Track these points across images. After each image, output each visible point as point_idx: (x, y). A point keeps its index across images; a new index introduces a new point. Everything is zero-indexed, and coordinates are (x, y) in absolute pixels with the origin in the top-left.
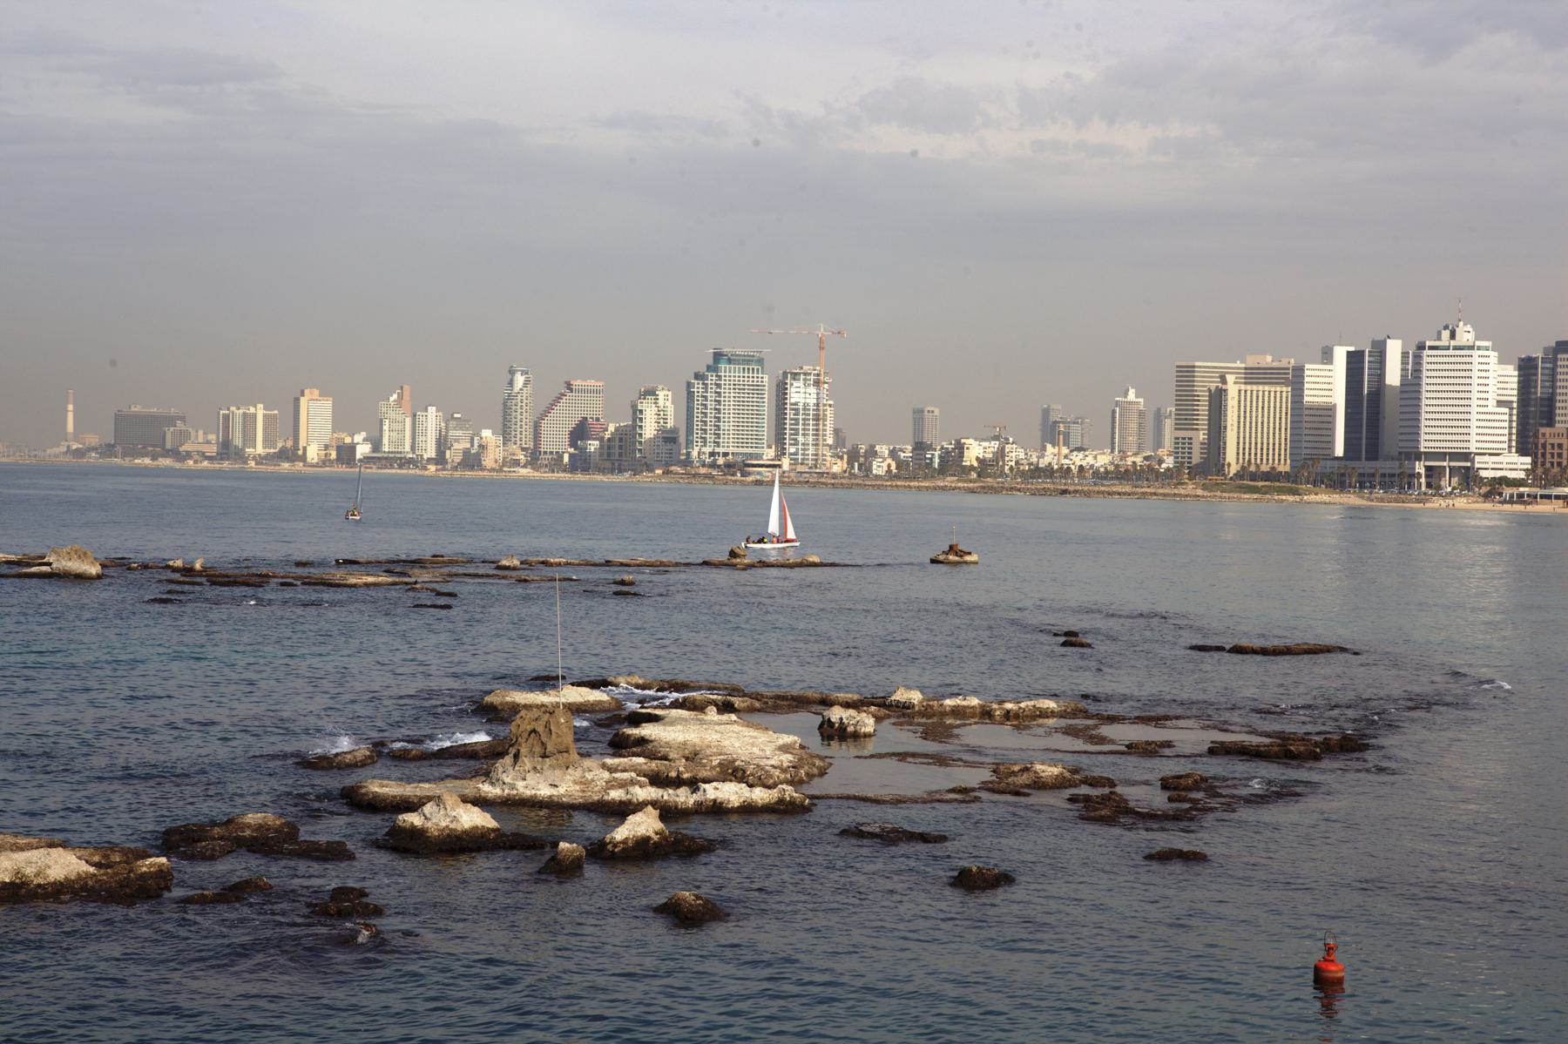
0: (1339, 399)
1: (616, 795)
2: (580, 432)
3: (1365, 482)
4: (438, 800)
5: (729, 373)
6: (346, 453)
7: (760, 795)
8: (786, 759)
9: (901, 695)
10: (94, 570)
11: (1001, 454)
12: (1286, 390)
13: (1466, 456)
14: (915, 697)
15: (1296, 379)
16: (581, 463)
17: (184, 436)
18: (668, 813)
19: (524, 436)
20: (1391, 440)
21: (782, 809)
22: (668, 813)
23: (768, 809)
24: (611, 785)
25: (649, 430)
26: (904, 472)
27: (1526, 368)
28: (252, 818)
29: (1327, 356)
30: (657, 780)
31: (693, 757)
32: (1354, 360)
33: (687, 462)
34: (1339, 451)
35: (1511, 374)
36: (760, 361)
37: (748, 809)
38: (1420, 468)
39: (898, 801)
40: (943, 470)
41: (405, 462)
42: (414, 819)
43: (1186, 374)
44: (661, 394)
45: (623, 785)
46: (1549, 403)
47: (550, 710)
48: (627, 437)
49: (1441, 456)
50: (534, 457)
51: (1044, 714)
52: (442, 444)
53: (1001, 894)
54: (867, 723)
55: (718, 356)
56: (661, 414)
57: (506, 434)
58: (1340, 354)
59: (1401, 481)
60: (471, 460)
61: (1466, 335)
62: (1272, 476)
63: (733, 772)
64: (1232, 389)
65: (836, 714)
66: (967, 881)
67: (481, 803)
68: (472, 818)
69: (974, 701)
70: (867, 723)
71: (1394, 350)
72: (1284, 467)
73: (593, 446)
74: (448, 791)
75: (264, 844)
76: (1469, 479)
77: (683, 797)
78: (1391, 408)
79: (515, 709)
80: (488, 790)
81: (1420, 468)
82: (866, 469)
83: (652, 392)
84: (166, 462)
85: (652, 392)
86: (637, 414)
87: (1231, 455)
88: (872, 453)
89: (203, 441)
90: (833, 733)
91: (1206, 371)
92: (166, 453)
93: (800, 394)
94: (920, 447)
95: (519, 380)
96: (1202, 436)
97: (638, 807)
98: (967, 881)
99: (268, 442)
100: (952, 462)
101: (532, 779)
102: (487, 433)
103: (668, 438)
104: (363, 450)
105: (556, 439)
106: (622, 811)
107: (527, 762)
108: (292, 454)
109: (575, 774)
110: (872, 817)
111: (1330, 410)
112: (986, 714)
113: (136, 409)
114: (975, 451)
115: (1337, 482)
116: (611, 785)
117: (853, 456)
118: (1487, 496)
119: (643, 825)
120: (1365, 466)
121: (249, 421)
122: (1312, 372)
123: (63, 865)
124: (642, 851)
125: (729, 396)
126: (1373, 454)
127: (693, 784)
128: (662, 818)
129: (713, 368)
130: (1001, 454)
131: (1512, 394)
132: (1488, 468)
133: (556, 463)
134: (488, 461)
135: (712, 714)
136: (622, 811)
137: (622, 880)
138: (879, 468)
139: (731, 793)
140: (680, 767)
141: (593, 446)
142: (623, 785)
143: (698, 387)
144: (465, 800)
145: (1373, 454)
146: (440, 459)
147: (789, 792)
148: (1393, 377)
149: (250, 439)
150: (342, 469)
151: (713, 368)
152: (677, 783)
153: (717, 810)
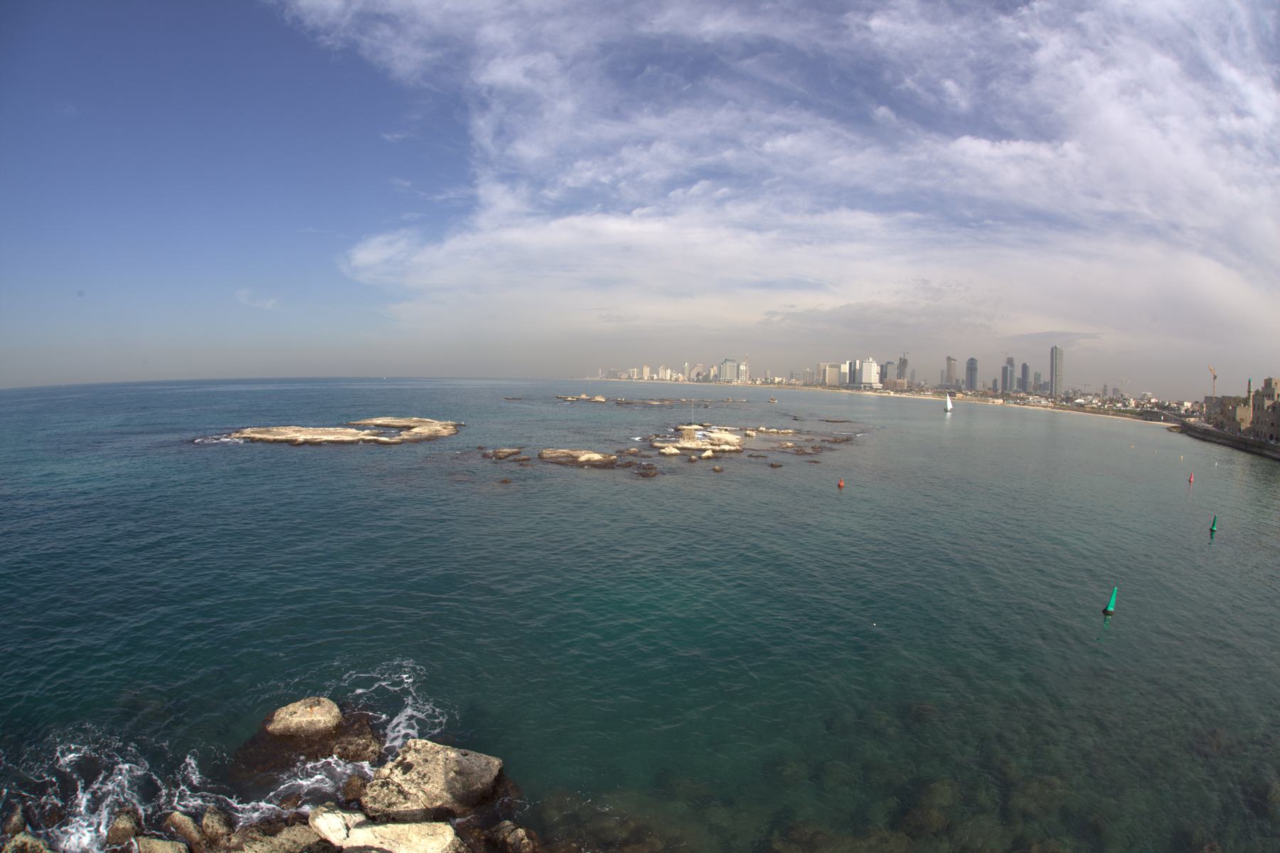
0: (848, 371)
1: (704, 447)
2: (698, 375)
3: (852, 388)
4: (668, 447)
5: (728, 363)
6: (652, 378)
7: (732, 448)
8: (738, 441)
9: (761, 429)
10: (604, 400)
11: (782, 380)
12: (838, 369)
13: (871, 384)
14: (764, 429)
15: (839, 368)
16: (698, 381)
17: (621, 375)
18: (714, 451)
19: (687, 374)
20: (857, 381)
21: (736, 451)
22: (714, 451)
23: (734, 451)
24: (703, 445)
25: (712, 374)
26: (763, 383)
27: (882, 367)
28: (633, 449)
29: (845, 363)
30: (712, 444)
31: (719, 440)
32: (850, 364)
33: (719, 381)
34: (848, 382)
35: (879, 368)
36: (734, 361)
37: (730, 451)
38: (862, 386)
39: (760, 450)
40: (771, 384)
41: (664, 380)
42: (663, 451)
43: (819, 365)
44: (715, 367)
45: (705, 445)
46: (886, 373)
47: (691, 430)
48: (708, 376)
49: (866, 383)
50: (689, 380)
51: (790, 433)
52: (671, 376)
53: (779, 469)
54: (754, 434)
55: (726, 360)
56: (714, 371)
57: (683, 374)
58: (848, 362)
59: (859, 389)
60: (677, 380)
61: (871, 360)
62: (835, 386)
63: (727, 443)
64: (827, 369)
65: (748, 432)
66: (772, 466)
67: (678, 448)
68: (675, 451)
69: (775, 430)
70: (754, 434)
71: (858, 362)
72: (837, 385)
73: (701, 377)
74: (669, 445)
75: (634, 454)
76: (871, 389)
77: (717, 448)
78: (857, 374)
79: (684, 430)
80: (678, 445)
81: (862, 386)
82: (755, 383)
83: (713, 367)
84: (618, 380)
85: (713, 367)
86: (709, 371)
87: (827, 381)
88: (756, 380)
89: (624, 376)
90: (747, 435)
91: (822, 367)
92: (619, 378)
93: (742, 367)
94: (766, 379)
95: (686, 364)
96: (821, 378)
97: (708, 450)
98: (772, 466)
99: (637, 376)
100: (772, 382)
101: (687, 443)
102: (680, 375)
103: (716, 376)
104: (655, 377)
105: (693, 375)
106: (704, 450)
107: (686, 440)
108: (642, 378)
109: (695, 443)
110: (756, 454)
111: (846, 373)
112: (778, 433)
113: (612, 369)
114: (777, 380)
115: (847, 388)
116: (703, 445)
117: (753, 380)
118: (875, 392)
119: (709, 453)
120: (852, 385)
121: (634, 372)
122: (842, 366)
123: (597, 457)
124: (708, 458)
125: (728, 369)
126: (854, 383)
127: (719, 445)
128: (713, 452)
129: (725, 362)
130: (782, 380)
131: (879, 372)
132: (875, 386)
133: (693, 381)
134: (680, 380)
135: (723, 431)
136: (704, 450)
137: (704, 463)
138: (758, 383)
139: (727, 447)
140: (716, 442)
141: (701, 377)
142: (705, 445)
143: (722, 366)
144: (674, 447)
145: (854, 383)
146: (671, 380)
147: (738, 447)
148: (858, 367)
149: (634, 375)
150: (651, 381)
151: (725, 362)
152: (716, 445)
153: (724, 451)
